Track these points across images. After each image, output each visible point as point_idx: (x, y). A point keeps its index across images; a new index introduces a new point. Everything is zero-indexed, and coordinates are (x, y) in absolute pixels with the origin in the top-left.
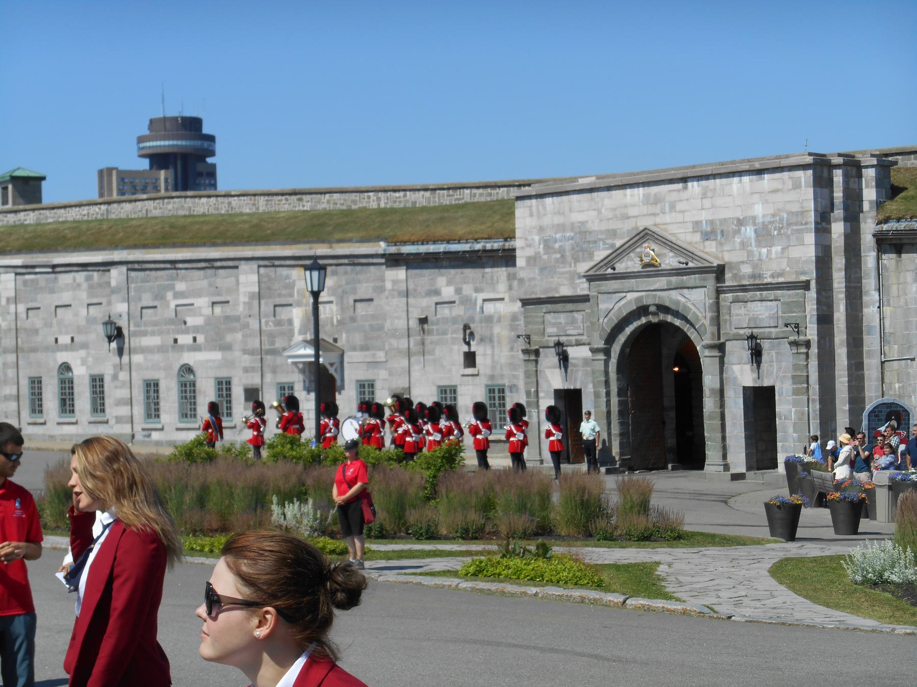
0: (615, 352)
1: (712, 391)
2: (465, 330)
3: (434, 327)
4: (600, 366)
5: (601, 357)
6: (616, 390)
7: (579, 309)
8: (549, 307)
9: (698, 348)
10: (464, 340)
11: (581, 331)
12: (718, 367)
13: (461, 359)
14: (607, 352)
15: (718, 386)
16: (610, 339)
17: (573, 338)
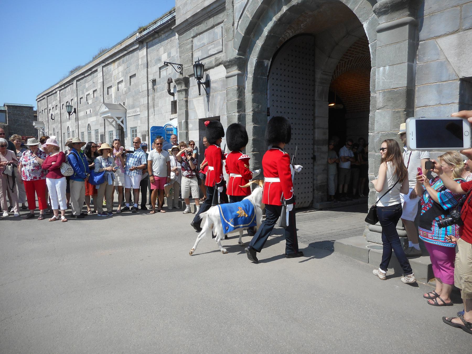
0: (252, 63)
1: (391, 94)
2: (169, 84)
3: (158, 86)
4: (234, 82)
5: (235, 71)
6: (251, 114)
7: (220, 20)
8: (195, 30)
9: (365, 25)
10: (169, 91)
11: (220, 48)
12: (405, 45)
13: (169, 107)
14: (241, 63)
15: (403, 83)
16: (245, 47)
17: (213, 58)
